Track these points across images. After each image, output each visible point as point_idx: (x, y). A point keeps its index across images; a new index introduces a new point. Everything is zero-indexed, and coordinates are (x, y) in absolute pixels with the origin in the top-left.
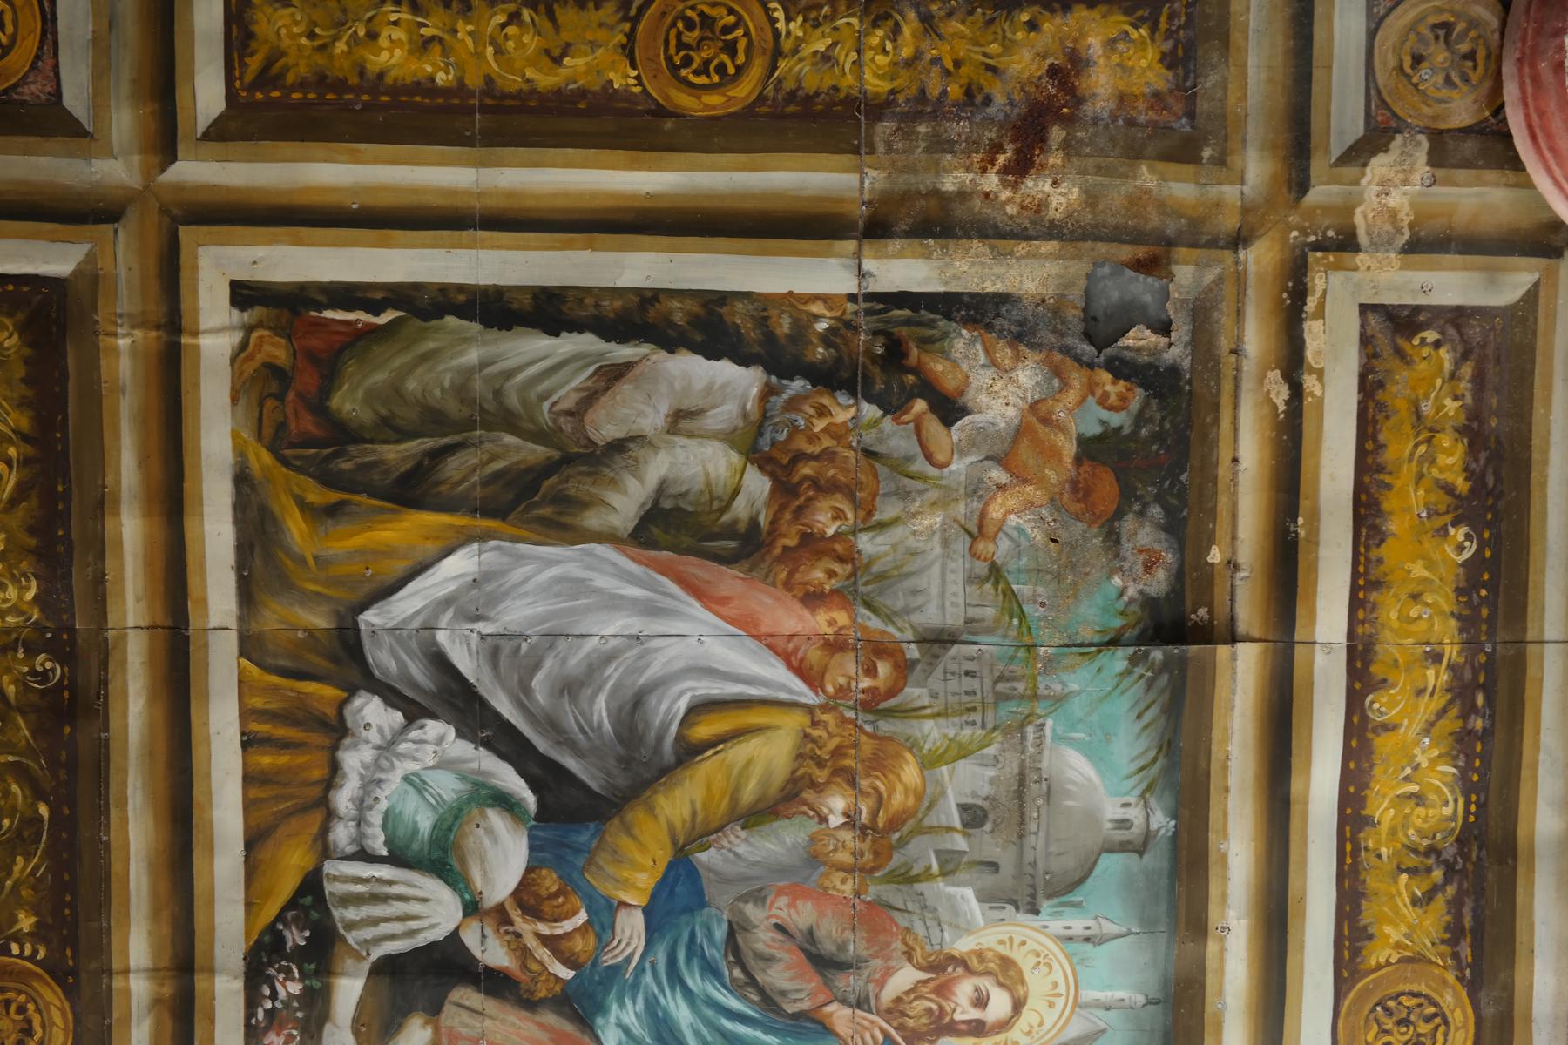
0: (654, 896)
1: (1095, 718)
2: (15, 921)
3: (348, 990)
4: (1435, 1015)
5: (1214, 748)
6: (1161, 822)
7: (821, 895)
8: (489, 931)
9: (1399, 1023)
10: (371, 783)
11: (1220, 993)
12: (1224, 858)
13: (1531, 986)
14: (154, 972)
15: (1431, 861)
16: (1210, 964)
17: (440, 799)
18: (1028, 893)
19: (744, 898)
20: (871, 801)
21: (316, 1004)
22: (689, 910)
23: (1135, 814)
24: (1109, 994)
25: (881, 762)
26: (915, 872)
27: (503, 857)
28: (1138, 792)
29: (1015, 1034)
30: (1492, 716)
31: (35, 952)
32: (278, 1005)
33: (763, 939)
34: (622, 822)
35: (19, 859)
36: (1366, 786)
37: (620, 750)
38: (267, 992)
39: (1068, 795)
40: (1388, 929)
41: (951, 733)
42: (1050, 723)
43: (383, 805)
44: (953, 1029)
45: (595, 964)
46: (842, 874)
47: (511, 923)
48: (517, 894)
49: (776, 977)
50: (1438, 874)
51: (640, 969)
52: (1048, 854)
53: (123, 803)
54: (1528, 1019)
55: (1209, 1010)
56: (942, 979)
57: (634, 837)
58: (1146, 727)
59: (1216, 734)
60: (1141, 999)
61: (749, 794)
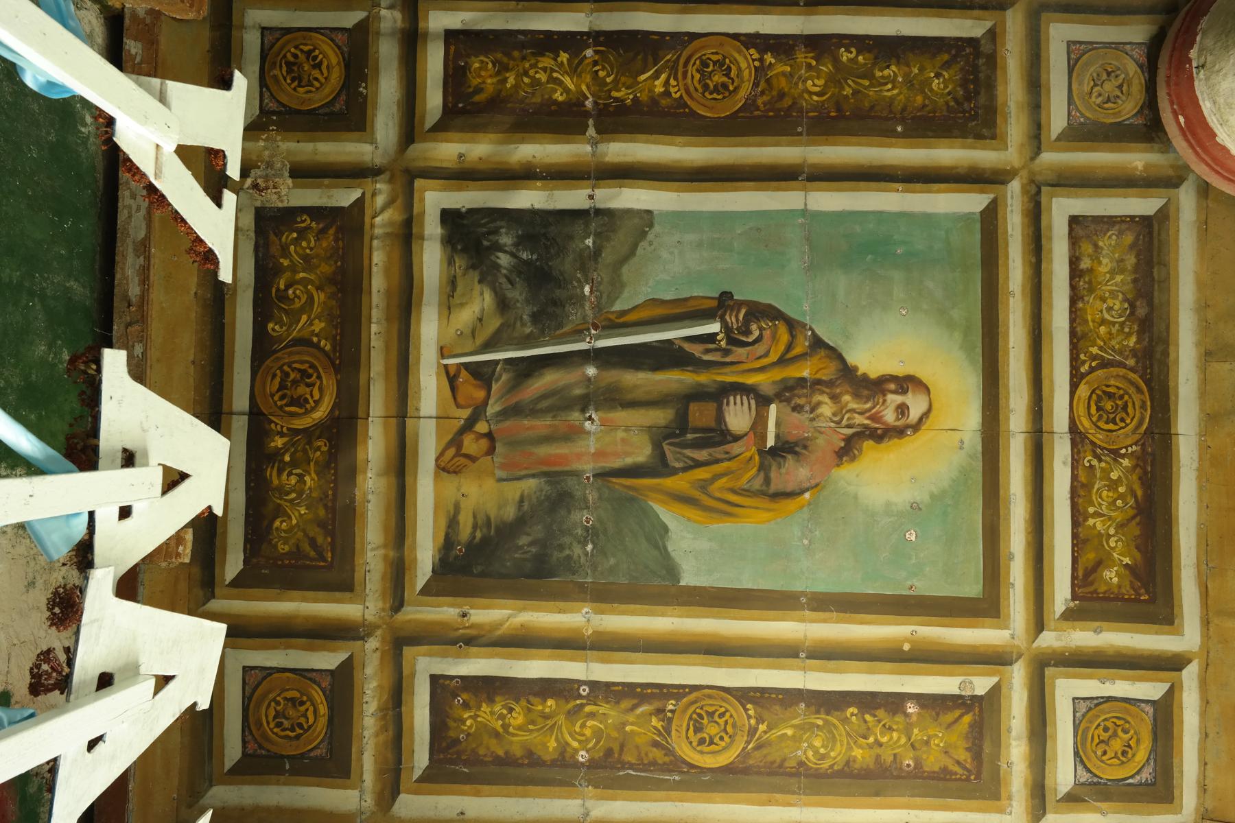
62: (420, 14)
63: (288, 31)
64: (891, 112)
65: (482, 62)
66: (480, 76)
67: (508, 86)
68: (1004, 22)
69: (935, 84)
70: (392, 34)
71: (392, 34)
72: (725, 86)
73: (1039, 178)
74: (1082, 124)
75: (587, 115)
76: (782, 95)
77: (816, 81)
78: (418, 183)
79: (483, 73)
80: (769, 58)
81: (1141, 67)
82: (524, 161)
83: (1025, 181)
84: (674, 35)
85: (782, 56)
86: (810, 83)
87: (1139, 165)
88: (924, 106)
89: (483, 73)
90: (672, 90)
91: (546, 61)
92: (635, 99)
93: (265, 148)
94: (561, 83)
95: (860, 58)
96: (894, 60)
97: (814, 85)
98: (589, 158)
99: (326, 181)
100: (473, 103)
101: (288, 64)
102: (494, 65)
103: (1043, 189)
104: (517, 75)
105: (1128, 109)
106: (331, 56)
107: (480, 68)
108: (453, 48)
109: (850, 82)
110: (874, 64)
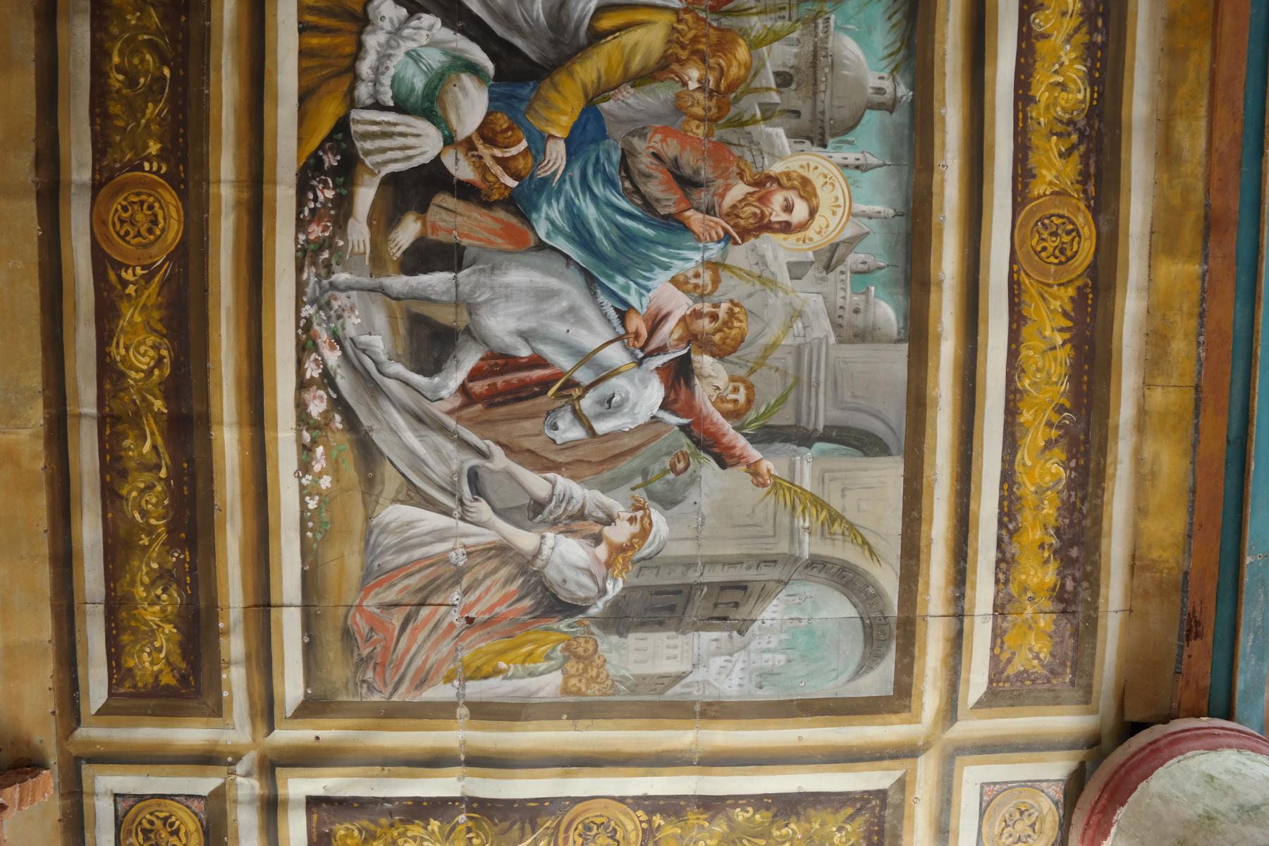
0: (572, 132)
1: (861, 16)
2: (146, 147)
3: (365, 196)
4: (1073, 230)
5: (937, 46)
6: (903, 91)
7: (683, 136)
8: (460, 156)
9: (1051, 234)
10: (384, 57)
11: (941, 209)
12: (943, 119)
14: (237, 183)
15: (1070, 129)
16: (935, 189)
17: (429, 67)
18: (817, 134)
19: (633, 134)
20: (716, 74)
21: (344, 205)
22: (596, 141)
23: (887, 85)
25: (723, 45)
26: (745, 118)
27: (471, 106)
28: (888, 70)
29: (810, 233)
30: (1107, 34)
31: (160, 168)
32: (319, 205)
33: (644, 162)
34: (552, 82)
35: (150, 105)
36: (1031, 75)
37: (551, 35)
38: (311, 196)
39: (845, 67)
40: (1044, 172)
41: (769, 24)
42: (833, 17)
43: (392, 72)
44: (768, 227)
45: (532, 177)
46: (697, 122)
47: (476, 150)
48: (480, 130)
49: (654, 189)
50: (1074, 137)
52: (832, 106)
53: (219, 69)
54: (1127, 235)
55: (935, 221)
56: (763, 191)
57: (558, 91)
58: (894, 26)
59: (938, 36)
60: (891, 212)
61: (635, 65)
62: (279, 782)
63: (142, 798)
65: (348, 829)
69: (836, 840)
70: (251, 802)
71: (251, 802)
80: (658, 820)
81: (1056, 803)
84: (552, 800)
85: (673, 818)
91: (415, 830)
95: (758, 817)
96: (794, 818)
101: (144, 831)
106: (189, 822)
107: (346, 836)
108: (315, 817)
110: (772, 823)
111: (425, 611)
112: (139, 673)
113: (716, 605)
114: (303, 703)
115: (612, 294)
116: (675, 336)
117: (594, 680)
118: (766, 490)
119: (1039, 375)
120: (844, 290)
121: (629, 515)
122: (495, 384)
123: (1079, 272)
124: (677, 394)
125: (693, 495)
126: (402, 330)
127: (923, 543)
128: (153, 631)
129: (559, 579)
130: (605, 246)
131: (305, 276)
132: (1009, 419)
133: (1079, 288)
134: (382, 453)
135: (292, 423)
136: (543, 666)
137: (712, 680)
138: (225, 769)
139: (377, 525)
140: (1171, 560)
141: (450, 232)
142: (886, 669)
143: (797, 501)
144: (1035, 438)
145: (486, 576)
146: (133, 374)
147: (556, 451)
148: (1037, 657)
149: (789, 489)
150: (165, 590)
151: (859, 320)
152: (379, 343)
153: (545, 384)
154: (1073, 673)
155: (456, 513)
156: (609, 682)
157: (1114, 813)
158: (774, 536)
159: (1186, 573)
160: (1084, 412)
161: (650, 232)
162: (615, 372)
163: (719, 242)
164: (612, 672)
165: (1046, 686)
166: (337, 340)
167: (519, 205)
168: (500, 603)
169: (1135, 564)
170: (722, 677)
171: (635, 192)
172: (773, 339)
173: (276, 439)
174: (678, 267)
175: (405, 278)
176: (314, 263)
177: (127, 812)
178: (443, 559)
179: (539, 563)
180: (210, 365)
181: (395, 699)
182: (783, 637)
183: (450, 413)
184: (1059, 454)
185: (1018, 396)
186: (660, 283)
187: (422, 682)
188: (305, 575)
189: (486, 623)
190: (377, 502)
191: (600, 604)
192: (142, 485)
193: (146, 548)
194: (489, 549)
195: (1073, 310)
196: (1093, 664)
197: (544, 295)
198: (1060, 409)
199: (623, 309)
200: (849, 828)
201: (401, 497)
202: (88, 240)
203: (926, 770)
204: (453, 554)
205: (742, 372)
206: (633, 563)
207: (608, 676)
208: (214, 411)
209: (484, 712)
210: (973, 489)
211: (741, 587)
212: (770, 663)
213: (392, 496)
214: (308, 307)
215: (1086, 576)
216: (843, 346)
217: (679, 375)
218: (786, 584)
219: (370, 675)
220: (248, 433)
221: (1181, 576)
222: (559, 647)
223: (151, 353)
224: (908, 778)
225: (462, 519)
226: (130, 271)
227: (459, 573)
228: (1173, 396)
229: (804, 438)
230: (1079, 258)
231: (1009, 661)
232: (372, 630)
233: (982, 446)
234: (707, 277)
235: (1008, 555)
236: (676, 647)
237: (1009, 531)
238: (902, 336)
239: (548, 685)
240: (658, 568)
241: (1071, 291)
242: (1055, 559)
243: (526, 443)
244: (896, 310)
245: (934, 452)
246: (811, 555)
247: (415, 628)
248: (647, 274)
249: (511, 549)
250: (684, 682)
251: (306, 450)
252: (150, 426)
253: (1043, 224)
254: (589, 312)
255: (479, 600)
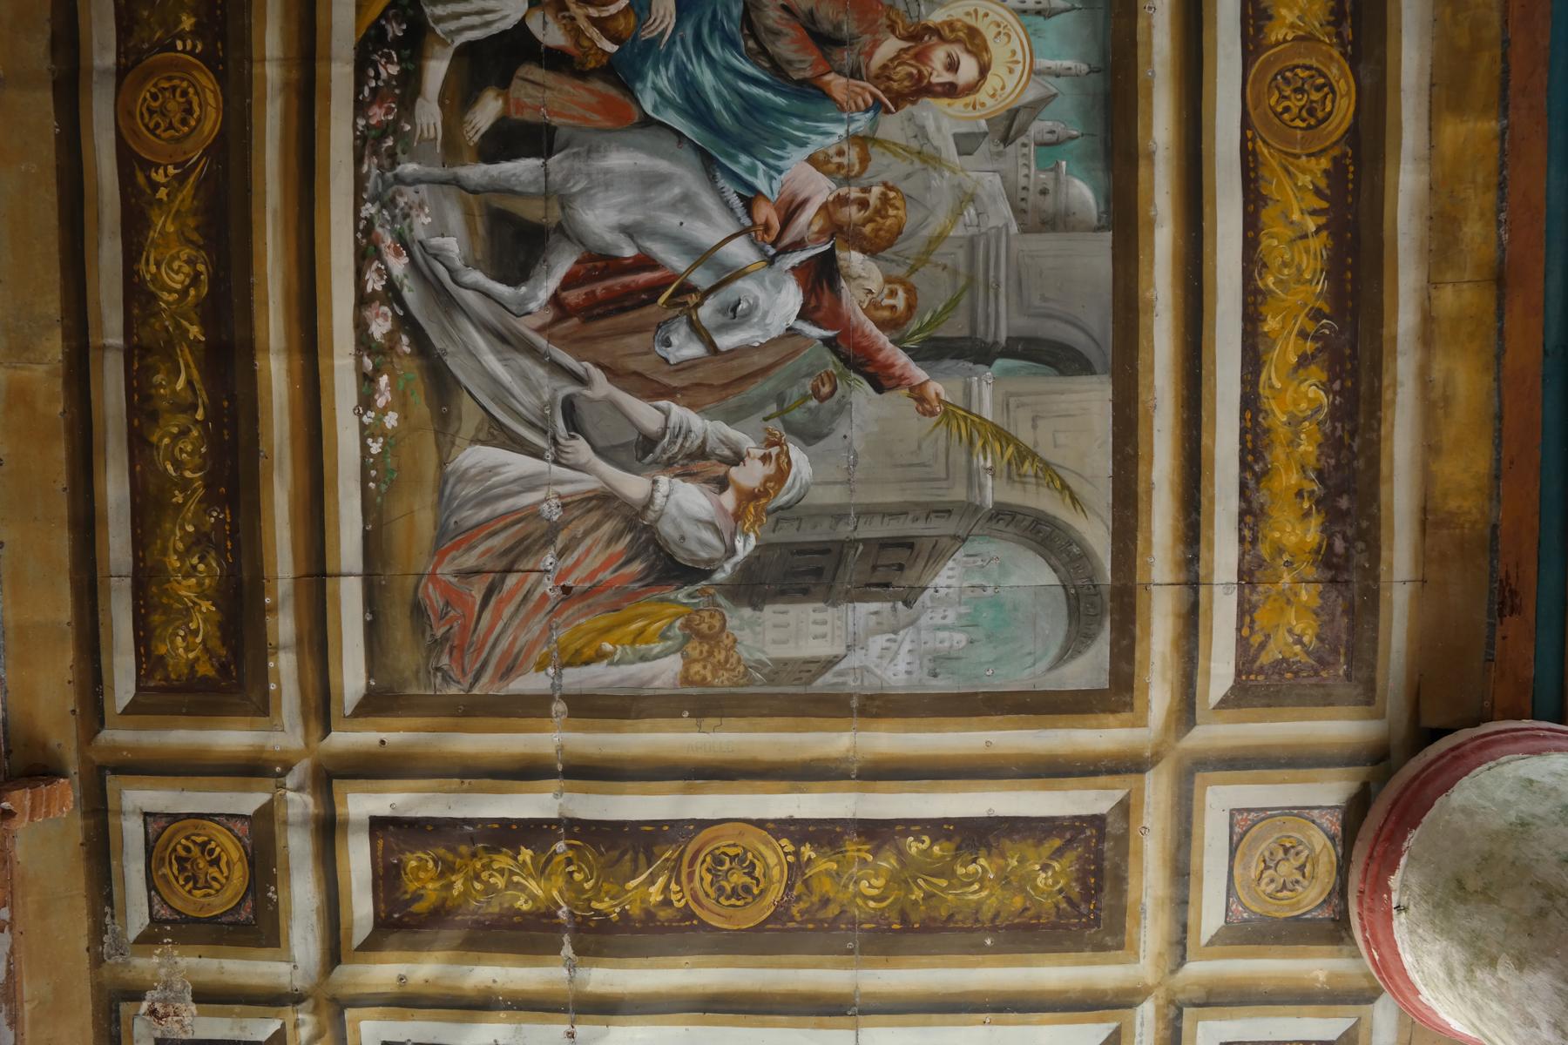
3: (436, 70)
4: (1323, 85)
8: (549, 18)
9: (1296, 91)
11: (1149, 62)
13: (1400, 60)
14: (285, 61)
16: (1141, 38)
21: (411, 83)
24: (1059, 63)
29: (982, 96)
31: (194, 46)
32: (381, 83)
33: (772, 16)
38: (372, 73)
40: (1284, 12)
45: (635, 39)
47: (567, 9)
49: (785, 48)
51: (672, 42)
60: (1084, 68)
62: (337, 799)
63: (175, 817)
64: (977, 920)
65: (420, 859)
66: (418, 879)
67: (455, 893)
68: (1141, 790)
69: (1040, 882)
70: (304, 823)
71: (304, 823)
72: (747, 889)
73: (1181, 997)
74: (1245, 921)
75: (559, 928)
76: (825, 902)
77: (874, 882)
78: (349, 1014)
79: (422, 875)
80: (807, 851)
81: (1332, 838)
82: (482, 986)
83: (1161, 1002)
85: (826, 849)
86: (864, 883)
87: (1322, 976)
88: (1026, 909)
89: (422, 875)
90: (674, 897)
91: (503, 861)
92: (624, 914)
93: (161, 965)
94: (523, 889)
95: (936, 849)
96: (983, 851)
97: (871, 886)
98: (565, 986)
99: (237, 1008)
100: (411, 914)
101: (180, 860)
102: (436, 865)
103: (1185, 1010)
104: (466, 880)
105: (1311, 897)
106: (231, 849)
107: (418, 868)
108: (381, 843)
109: (920, 882)
110: (955, 857)
111: (512, 580)
112: (171, 662)
113: (874, 568)
114: (366, 697)
115: (735, 178)
116: (815, 228)
117: (722, 665)
118: (935, 419)
119: (1286, 271)
120: (1028, 166)
121: (761, 452)
122: (593, 292)
123: (1334, 138)
124: (818, 299)
125: (842, 428)
126: (481, 230)
127: (1141, 487)
128: (188, 609)
129: (675, 535)
130: (726, 118)
131: (365, 168)
132: (1249, 328)
133: (1335, 160)
134: (458, 382)
135: (350, 346)
136: (658, 647)
137: (872, 666)
138: (272, 781)
139: (453, 472)
140: (1474, 511)
141: (537, 109)
142: (1100, 650)
143: (975, 434)
144: (1284, 352)
145: (586, 534)
146: (165, 295)
147: (668, 373)
148: (1299, 641)
149: (965, 418)
150: (201, 560)
151: (1048, 203)
152: (453, 246)
153: (654, 290)
154: (1349, 663)
155: (549, 455)
156: (741, 669)
157: (1404, 838)
158: (947, 478)
159: (1495, 527)
160: (1348, 319)
161: (780, 101)
162: (741, 273)
163: (867, 111)
164: (745, 655)
165: (1314, 680)
166: (403, 243)
167: (619, 74)
168: (604, 566)
169: (1429, 519)
170: (885, 662)
171: (761, 53)
172: (939, 230)
173: (332, 368)
174: (817, 143)
175: (484, 167)
176: (375, 153)
177: (159, 836)
178: (533, 513)
179: (651, 515)
180: (254, 279)
181: (476, 691)
182: (963, 610)
183: (540, 330)
184: (1317, 373)
185: (1260, 298)
186: (795, 162)
187: (509, 670)
188: (366, 536)
189: (585, 594)
190: (453, 444)
191: (728, 567)
192: (175, 430)
193: (179, 507)
194: (590, 499)
195: (1329, 186)
196: (1375, 651)
197: (651, 181)
198: (1316, 315)
199: (749, 195)
200: (1057, 866)
201: (482, 436)
202: (112, 135)
203: (1156, 789)
204: (545, 506)
205: (900, 272)
206: (768, 514)
207: (739, 660)
208: (259, 334)
209: (587, 708)
210: (1204, 419)
211: (906, 544)
212: (947, 644)
213: (472, 433)
214: (369, 205)
215: (1361, 535)
216: (1028, 236)
217: (821, 278)
218: (964, 541)
219: (445, 661)
220: (298, 361)
221: (1487, 532)
222: (678, 624)
223: (186, 269)
224: (1132, 801)
225: (556, 462)
226: (161, 171)
227: (554, 529)
228: (1469, 295)
229: (980, 352)
230: (1334, 120)
231: (1263, 646)
232: (447, 604)
233: (1214, 362)
234: (853, 155)
235: (1255, 505)
236: (825, 623)
237: (1254, 473)
238: (1103, 222)
239: (664, 671)
240: (800, 519)
241: (1325, 163)
242: (1318, 512)
243: (633, 364)
244: (1095, 190)
245: (1152, 370)
246: (995, 503)
247: (500, 601)
248: (779, 152)
249: (615, 498)
250: (837, 668)
251: (367, 380)
252: (185, 357)
253: (1285, 79)
254: (708, 200)
255: (577, 564)
